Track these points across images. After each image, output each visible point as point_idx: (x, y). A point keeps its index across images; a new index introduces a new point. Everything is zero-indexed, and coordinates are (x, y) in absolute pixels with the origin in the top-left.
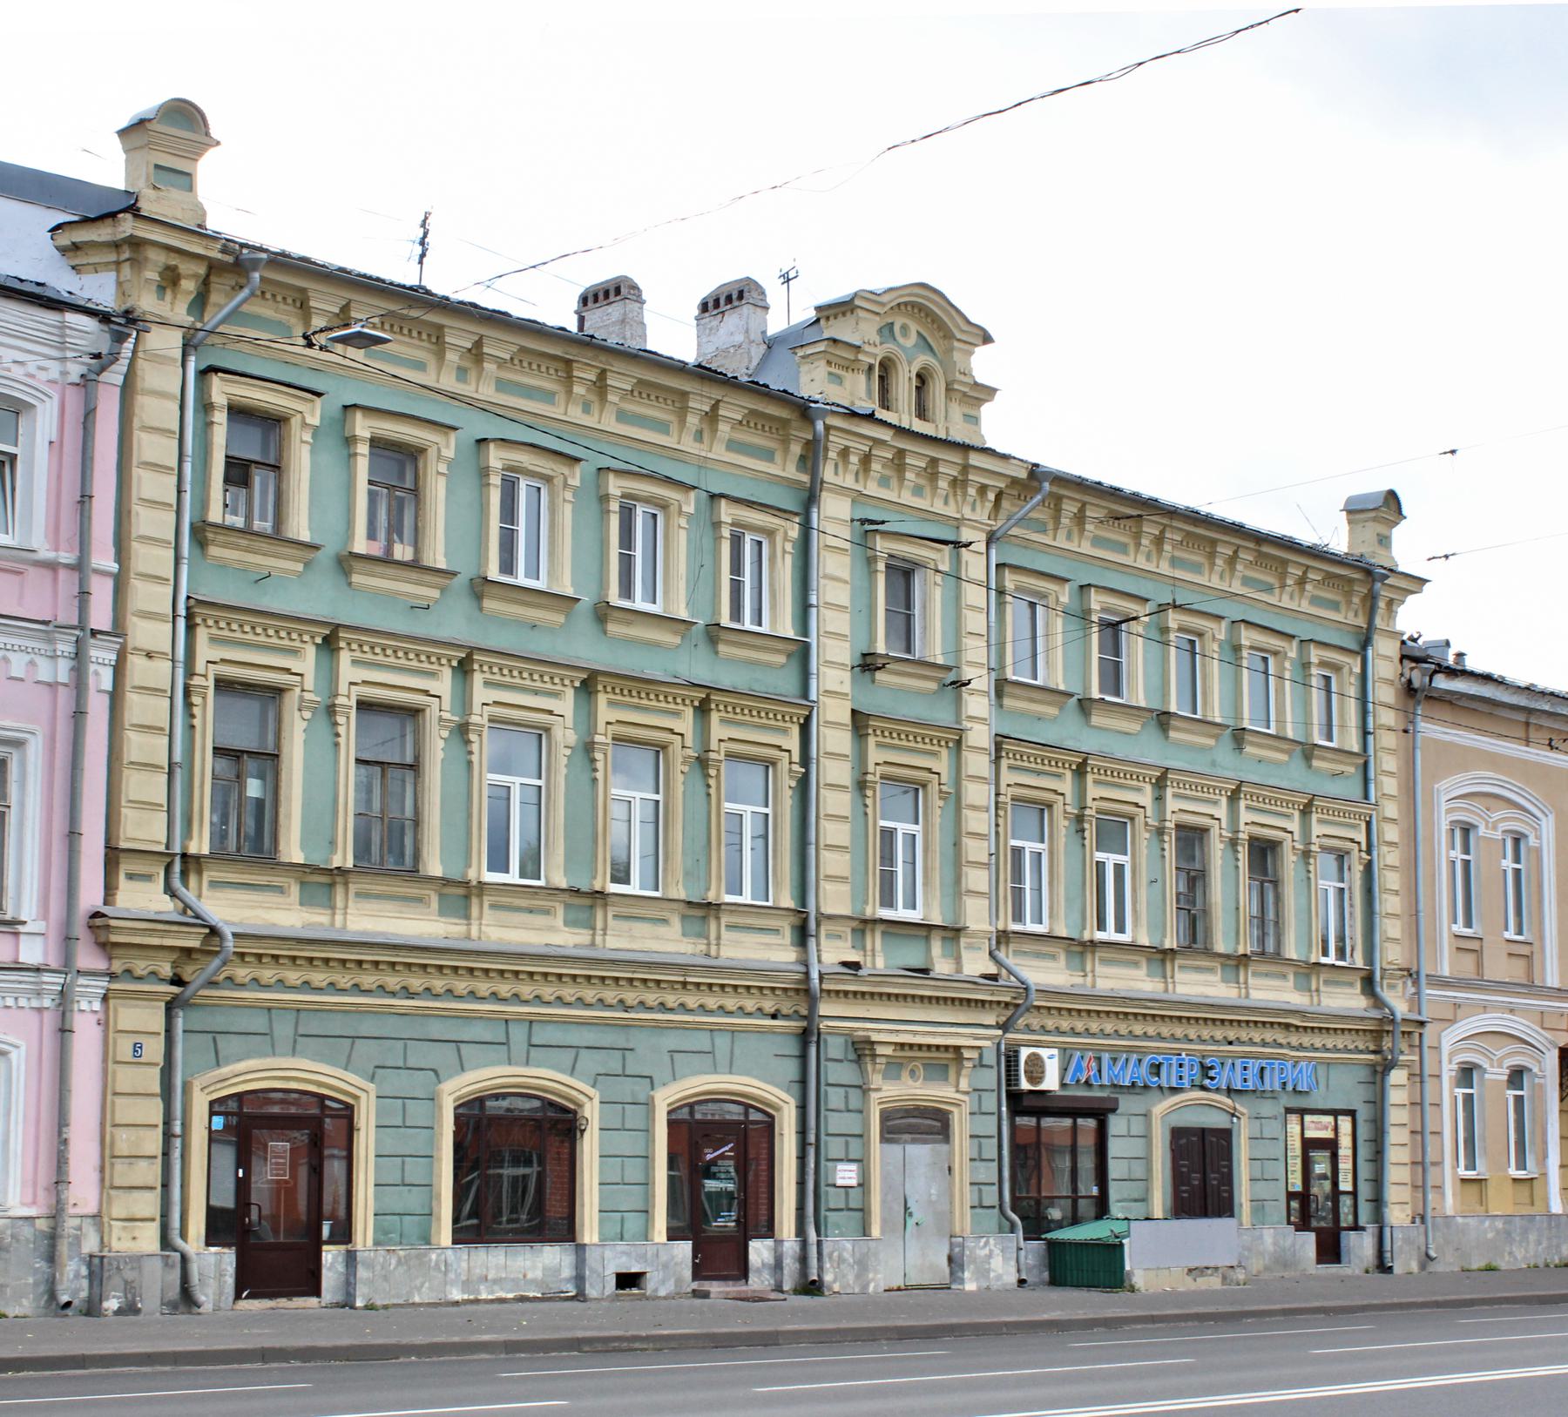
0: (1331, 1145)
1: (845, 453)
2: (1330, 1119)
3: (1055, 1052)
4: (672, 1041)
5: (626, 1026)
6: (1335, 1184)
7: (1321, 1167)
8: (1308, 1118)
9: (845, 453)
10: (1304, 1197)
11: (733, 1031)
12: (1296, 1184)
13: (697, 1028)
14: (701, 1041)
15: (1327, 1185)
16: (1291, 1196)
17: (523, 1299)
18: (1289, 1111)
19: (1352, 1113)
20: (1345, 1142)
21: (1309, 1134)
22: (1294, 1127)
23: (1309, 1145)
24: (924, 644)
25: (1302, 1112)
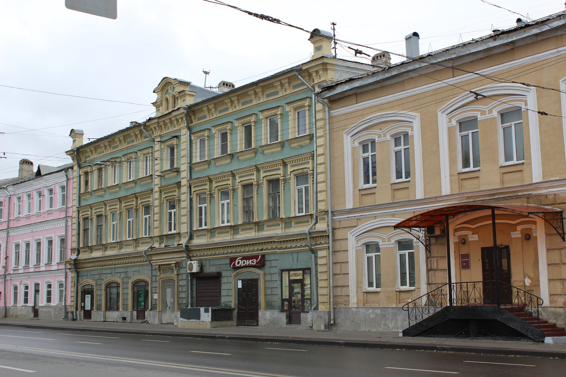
0: (301, 282)
1: (155, 128)
2: (301, 272)
3: (195, 261)
4: (133, 269)
5: (127, 267)
6: (303, 295)
7: (297, 290)
8: (291, 272)
9: (155, 128)
10: (289, 300)
11: (143, 265)
12: (286, 295)
13: (136, 266)
14: (137, 269)
15: (299, 296)
16: (283, 300)
17: (114, 321)
18: (283, 271)
19: (309, 269)
20: (307, 281)
21: (291, 278)
22: (285, 275)
23: (291, 282)
24: (177, 164)
25: (289, 270)
